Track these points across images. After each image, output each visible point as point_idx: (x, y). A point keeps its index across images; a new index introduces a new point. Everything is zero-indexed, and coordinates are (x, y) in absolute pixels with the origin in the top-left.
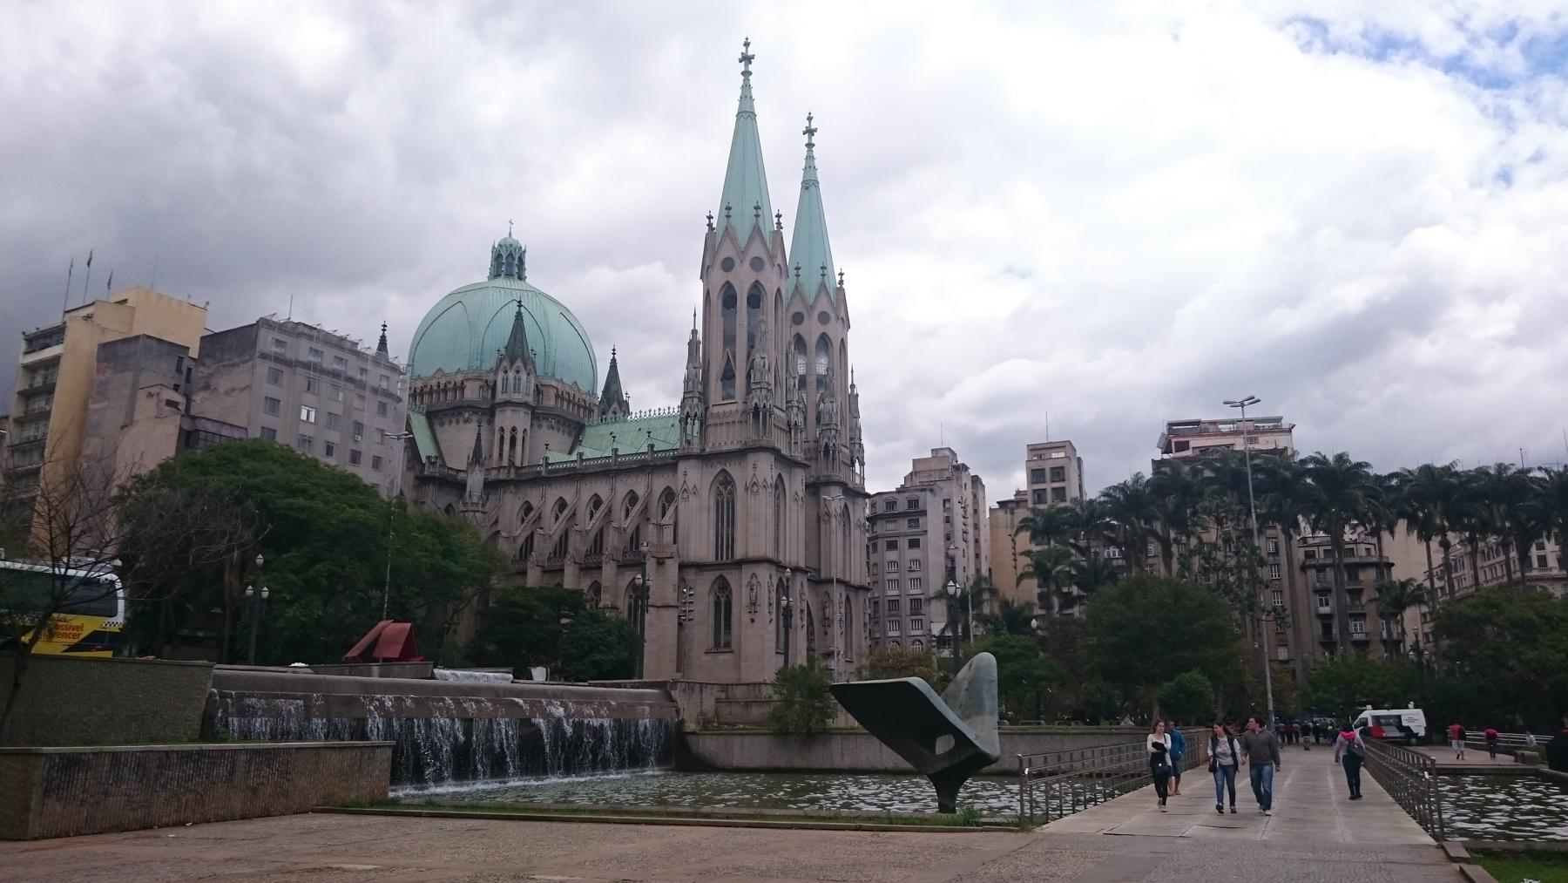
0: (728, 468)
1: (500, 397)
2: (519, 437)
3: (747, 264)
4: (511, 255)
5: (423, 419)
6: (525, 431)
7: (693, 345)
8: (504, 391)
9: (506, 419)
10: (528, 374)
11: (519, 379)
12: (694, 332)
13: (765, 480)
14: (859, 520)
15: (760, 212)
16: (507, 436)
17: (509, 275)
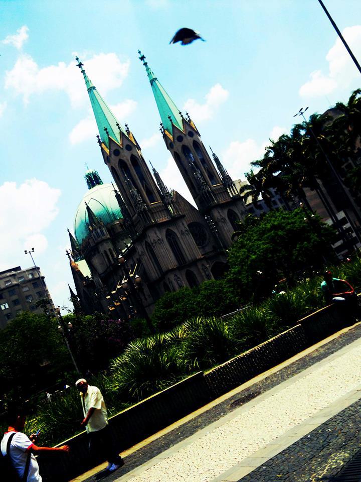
0: (146, 240)
1: (96, 242)
2: (108, 253)
3: (113, 156)
4: (90, 178)
5: (84, 261)
6: (110, 249)
7: (118, 196)
8: (96, 240)
9: (102, 249)
10: (100, 228)
11: (98, 232)
12: (116, 191)
13: (154, 240)
14: (242, 211)
15: (108, 131)
16: (104, 255)
17: (93, 185)
